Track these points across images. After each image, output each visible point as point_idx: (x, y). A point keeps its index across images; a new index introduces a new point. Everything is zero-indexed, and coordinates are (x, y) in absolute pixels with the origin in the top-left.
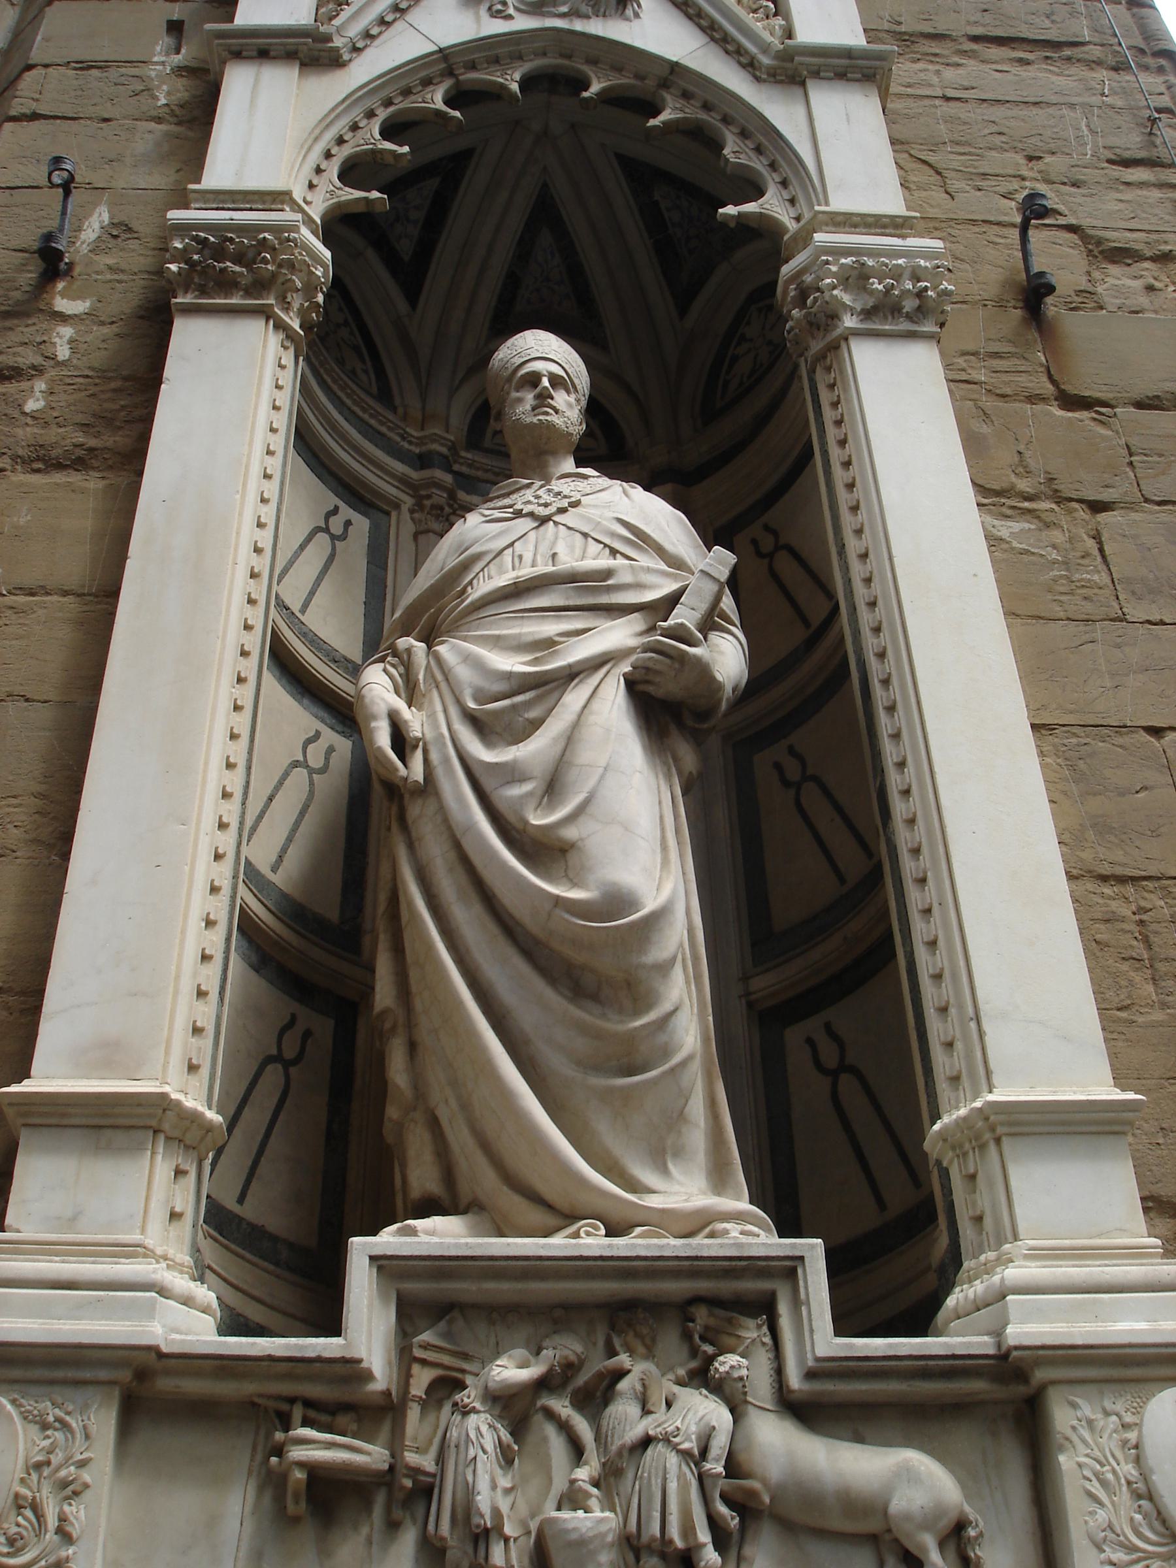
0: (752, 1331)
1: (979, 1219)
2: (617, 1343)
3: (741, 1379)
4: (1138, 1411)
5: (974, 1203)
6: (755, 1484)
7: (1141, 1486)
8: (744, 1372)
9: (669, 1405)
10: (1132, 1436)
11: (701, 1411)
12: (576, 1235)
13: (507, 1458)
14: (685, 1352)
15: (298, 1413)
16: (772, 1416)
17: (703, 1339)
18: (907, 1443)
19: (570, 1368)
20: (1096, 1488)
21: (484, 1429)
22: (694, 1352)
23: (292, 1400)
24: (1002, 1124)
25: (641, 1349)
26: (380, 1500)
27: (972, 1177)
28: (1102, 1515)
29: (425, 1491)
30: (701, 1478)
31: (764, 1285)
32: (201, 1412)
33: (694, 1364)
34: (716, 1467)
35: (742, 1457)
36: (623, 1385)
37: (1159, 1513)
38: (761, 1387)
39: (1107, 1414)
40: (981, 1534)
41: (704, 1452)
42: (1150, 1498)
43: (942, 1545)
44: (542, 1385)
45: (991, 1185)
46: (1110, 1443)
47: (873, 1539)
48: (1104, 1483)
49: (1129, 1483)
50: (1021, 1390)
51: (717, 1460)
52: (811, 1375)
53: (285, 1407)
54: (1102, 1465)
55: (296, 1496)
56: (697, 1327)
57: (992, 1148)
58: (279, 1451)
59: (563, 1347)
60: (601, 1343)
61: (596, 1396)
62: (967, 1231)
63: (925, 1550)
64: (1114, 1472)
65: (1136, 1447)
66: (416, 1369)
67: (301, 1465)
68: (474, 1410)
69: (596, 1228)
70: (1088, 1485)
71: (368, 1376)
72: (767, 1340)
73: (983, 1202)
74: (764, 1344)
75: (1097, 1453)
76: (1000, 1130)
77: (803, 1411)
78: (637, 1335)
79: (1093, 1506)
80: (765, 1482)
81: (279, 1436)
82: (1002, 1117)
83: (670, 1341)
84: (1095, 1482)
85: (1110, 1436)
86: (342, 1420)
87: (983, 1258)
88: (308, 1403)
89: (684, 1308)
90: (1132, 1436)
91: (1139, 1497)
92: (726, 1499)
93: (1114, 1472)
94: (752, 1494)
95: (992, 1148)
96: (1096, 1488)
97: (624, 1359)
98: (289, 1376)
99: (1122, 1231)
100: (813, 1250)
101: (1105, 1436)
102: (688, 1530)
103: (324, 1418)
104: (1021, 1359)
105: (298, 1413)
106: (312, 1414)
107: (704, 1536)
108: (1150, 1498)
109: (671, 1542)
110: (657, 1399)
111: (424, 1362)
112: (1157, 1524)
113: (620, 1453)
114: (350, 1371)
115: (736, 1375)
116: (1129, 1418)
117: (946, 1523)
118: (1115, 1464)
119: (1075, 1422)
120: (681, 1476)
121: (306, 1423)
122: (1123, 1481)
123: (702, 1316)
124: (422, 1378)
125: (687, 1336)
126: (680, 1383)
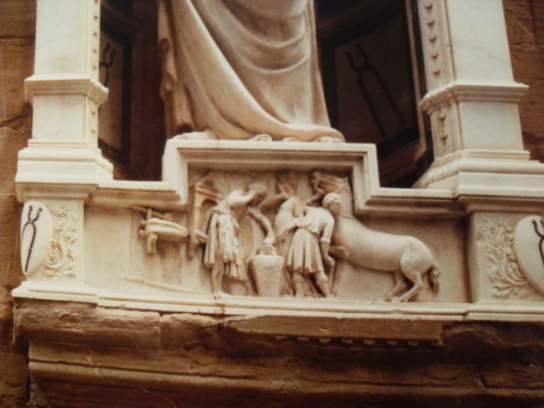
0: (341, 183)
1: (444, 139)
2: (281, 187)
3: (338, 204)
4: (514, 225)
5: (443, 132)
6: (342, 248)
7: (513, 257)
8: (339, 201)
9: (305, 214)
10: (510, 236)
11: (319, 217)
12: (259, 140)
13: (237, 233)
14: (310, 192)
15: (150, 212)
16: (350, 221)
17: (319, 187)
18: (408, 234)
19: (261, 197)
20: (492, 256)
21: (228, 221)
22: (314, 192)
23: (147, 208)
24: (460, 95)
25: (292, 191)
26: (183, 249)
27: (442, 120)
28: (494, 268)
29: (203, 246)
30: (320, 244)
31: (348, 164)
32: (110, 211)
33: (315, 197)
34: (326, 239)
35: (337, 236)
36: (285, 205)
37: (520, 268)
38: (346, 208)
39: (500, 225)
40: (440, 274)
41: (322, 234)
42: (516, 261)
43: (423, 276)
44: (250, 204)
45: (452, 123)
46: (500, 237)
47: (392, 274)
48: (495, 253)
49: (507, 255)
50: (461, 213)
51: (328, 237)
52: (369, 203)
53: (144, 210)
54: (496, 247)
55: (152, 245)
56: (316, 182)
57: (454, 106)
58: (143, 227)
59: (258, 187)
60: (273, 187)
61: (272, 209)
62: (438, 144)
63: (415, 277)
64: (501, 250)
65: (512, 240)
66: (197, 195)
67: (155, 233)
68: (223, 213)
69: (267, 137)
70: (489, 255)
71: (178, 198)
72: (348, 188)
73: (447, 130)
74: (347, 189)
75: (494, 242)
76: (459, 98)
77: (364, 218)
78: (291, 185)
79: (491, 264)
80: (346, 246)
81: (143, 222)
82: (461, 92)
83: (303, 187)
84: (493, 254)
85: (501, 236)
86: (168, 215)
87: (446, 156)
88: (154, 209)
89: (309, 174)
90: (510, 236)
91: (512, 261)
92: (330, 254)
93: (501, 250)
94: (342, 252)
95: (454, 106)
96: (492, 256)
97: (284, 194)
98: (147, 197)
99: (513, 147)
100: (370, 150)
101: (499, 235)
102: (314, 265)
103: (160, 215)
104: (462, 200)
105: (150, 212)
106: (155, 213)
107: (321, 268)
108: (516, 261)
109: (307, 269)
110: (299, 211)
111: (200, 193)
112: (518, 273)
113: (284, 234)
114: (171, 195)
115: (336, 202)
116: (509, 228)
117: (425, 268)
118: (501, 247)
119: (485, 229)
120: (312, 243)
121: (153, 216)
122: (505, 255)
123: (318, 176)
124: (199, 200)
125: (311, 185)
126: (309, 205)
